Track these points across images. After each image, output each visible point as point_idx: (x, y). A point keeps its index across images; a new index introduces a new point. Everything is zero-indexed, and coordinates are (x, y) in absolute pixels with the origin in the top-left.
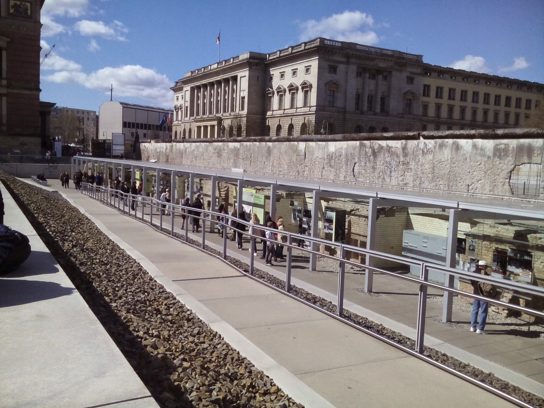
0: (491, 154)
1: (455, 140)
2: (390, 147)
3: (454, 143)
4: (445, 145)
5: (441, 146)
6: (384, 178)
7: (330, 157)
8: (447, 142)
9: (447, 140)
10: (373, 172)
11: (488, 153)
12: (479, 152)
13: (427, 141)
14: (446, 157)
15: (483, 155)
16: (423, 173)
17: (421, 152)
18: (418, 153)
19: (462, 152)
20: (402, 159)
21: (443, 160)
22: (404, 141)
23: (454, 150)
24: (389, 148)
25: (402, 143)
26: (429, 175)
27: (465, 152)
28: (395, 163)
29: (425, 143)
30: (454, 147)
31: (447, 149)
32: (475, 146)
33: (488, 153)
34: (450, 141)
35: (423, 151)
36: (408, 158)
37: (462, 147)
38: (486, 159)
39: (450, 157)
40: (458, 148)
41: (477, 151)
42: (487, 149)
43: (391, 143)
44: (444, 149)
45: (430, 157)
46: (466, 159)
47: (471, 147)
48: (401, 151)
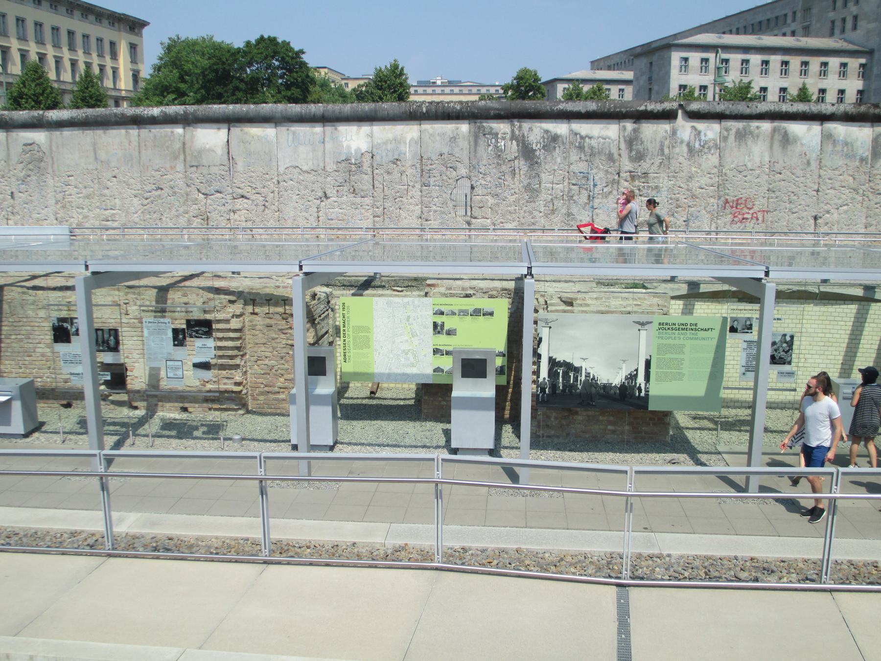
0: (867, 154)
1: (777, 124)
2: (582, 138)
3: (775, 130)
4: (751, 133)
5: (741, 136)
6: (569, 214)
7: (351, 167)
8: (758, 127)
9: (754, 124)
10: (532, 199)
11: (860, 152)
12: (839, 148)
13: (701, 125)
14: (757, 159)
15: (850, 156)
16: (694, 197)
17: (685, 149)
18: (677, 150)
19: (798, 149)
20: (627, 165)
21: (749, 166)
22: (629, 125)
23: (776, 144)
24: (581, 144)
25: (625, 128)
26: (712, 200)
27: (805, 149)
28: (601, 174)
29: (693, 127)
30: (778, 137)
31: (760, 143)
32: (827, 137)
33: (860, 152)
34: (766, 126)
35: (691, 150)
36: (645, 165)
37: (796, 139)
38: (857, 163)
39: (767, 159)
40: (787, 140)
41: (835, 146)
42: (859, 143)
43: (584, 128)
44: (749, 143)
45: (713, 159)
46: (808, 163)
47: (818, 138)
48: (623, 146)
